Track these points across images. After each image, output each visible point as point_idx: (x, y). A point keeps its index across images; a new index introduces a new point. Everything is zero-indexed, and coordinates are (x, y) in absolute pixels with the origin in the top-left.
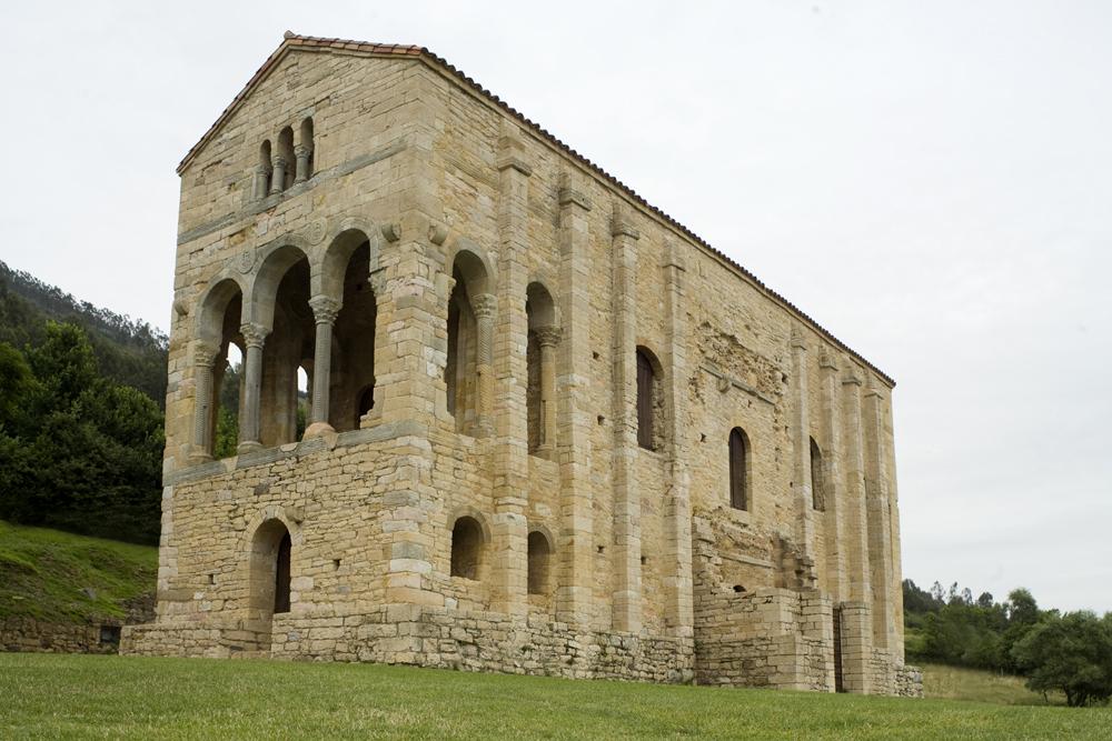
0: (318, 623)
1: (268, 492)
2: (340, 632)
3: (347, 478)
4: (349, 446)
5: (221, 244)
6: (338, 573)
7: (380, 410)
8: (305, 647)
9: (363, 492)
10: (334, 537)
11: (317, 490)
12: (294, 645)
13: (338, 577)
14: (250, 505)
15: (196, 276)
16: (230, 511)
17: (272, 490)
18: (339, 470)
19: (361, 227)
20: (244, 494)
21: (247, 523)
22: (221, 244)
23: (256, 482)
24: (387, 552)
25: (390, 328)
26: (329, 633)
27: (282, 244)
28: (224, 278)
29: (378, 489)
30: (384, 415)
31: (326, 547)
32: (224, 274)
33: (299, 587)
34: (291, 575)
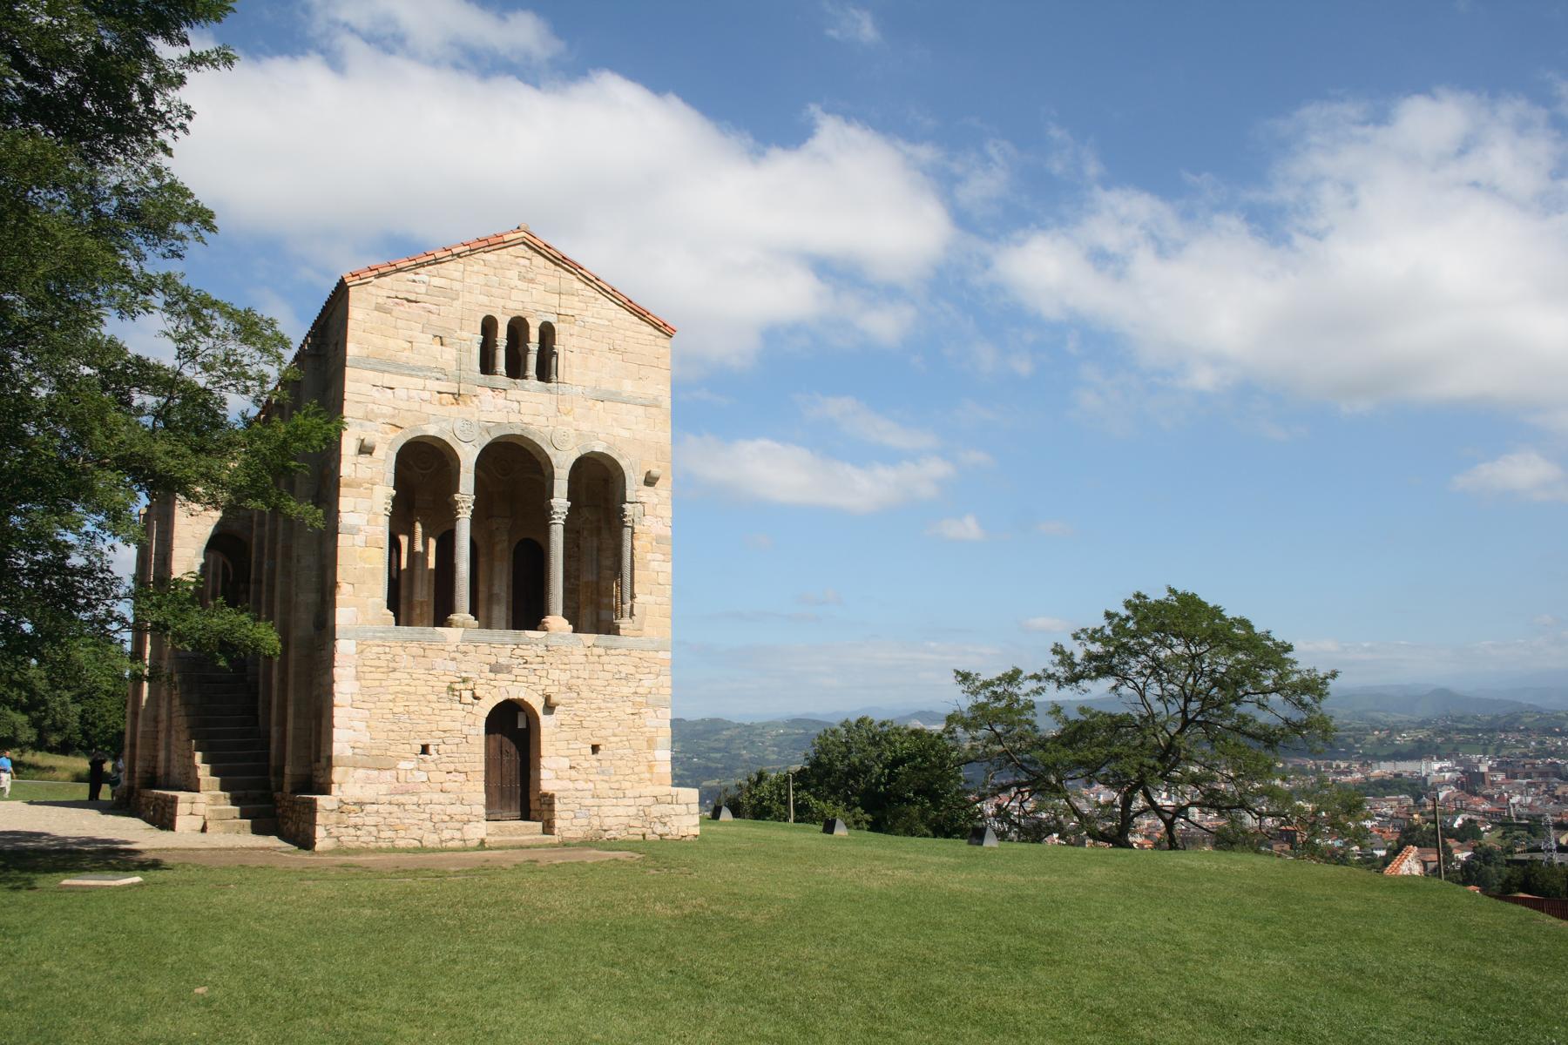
0: (608, 802)
2: (632, 811)
3: (609, 676)
4: (607, 648)
5: (426, 395)
6: (599, 755)
7: (642, 624)
8: (596, 822)
9: (626, 691)
11: (574, 681)
12: (584, 821)
15: (384, 416)
17: (516, 671)
19: (615, 456)
20: (474, 666)
23: (493, 660)
24: (651, 743)
25: (649, 556)
26: (621, 811)
27: (518, 432)
28: (431, 433)
29: (640, 690)
30: (646, 629)
32: (431, 430)
33: (554, 766)
34: (543, 753)
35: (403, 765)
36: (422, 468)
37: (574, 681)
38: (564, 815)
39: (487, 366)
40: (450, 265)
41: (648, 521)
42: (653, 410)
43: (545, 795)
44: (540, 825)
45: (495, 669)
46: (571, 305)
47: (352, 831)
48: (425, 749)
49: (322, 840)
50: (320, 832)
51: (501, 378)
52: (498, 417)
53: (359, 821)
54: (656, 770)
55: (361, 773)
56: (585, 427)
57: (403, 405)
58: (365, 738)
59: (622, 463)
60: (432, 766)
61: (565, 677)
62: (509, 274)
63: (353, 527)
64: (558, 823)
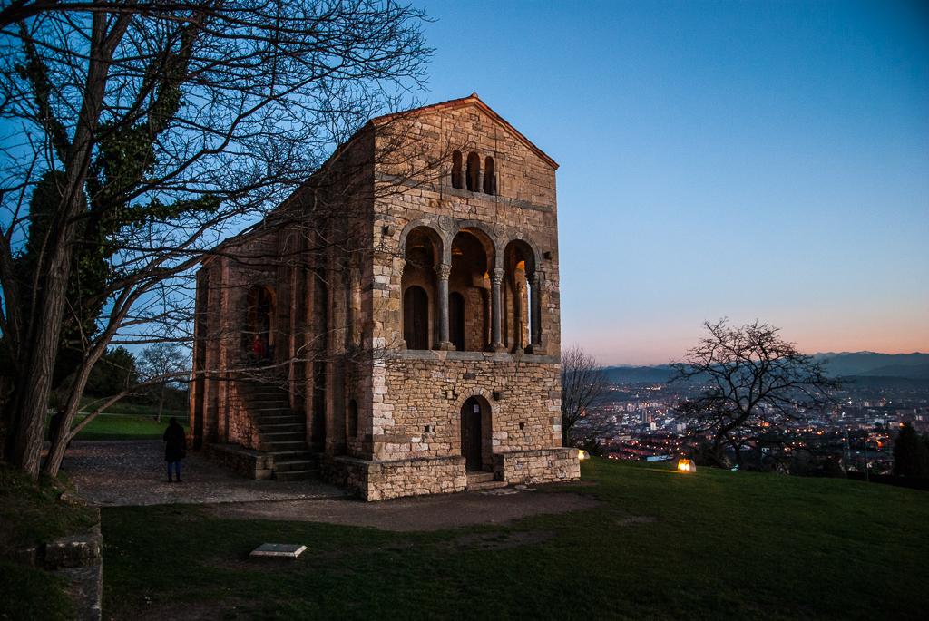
0: (532, 459)
1: (474, 379)
4: (527, 363)
5: (423, 200)
10: (521, 410)
11: (510, 384)
12: (520, 472)
13: (524, 433)
14: (459, 384)
16: (442, 386)
18: (522, 375)
21: (457, 396)
22: (423, 200)
23: (465, 372)
24: (551, 422)
29: (545, 388)
31: (516, 416)
32: (426, 222)
33: (499, 438)
34: (494, 429)
35: (415, 440)
36: (421, 245)
37: (510, 384)
38: (510, 469)
39: (456, 184)
40: (434, 118)
41: (548, 283)
42: (548, 215)
43: (497, 455)
44: (491, 475)
45: (467, 376)
46: (502, 147)
47: (389, 486)
48: (427, 429)
49: (373, 495)
50: (371, 487)
51: (464, 192)
52: (463, 216)
53: (394, 479)
54: (554, 438)
55: (390, 446)
56: (512, 224)
57: (409, 206)
58: (392, 424)
59: (533, 247)
60: (431, 440)
61: (504, 381)
62: (467, 125)
63: (382, 284)
64: (506, 474)
